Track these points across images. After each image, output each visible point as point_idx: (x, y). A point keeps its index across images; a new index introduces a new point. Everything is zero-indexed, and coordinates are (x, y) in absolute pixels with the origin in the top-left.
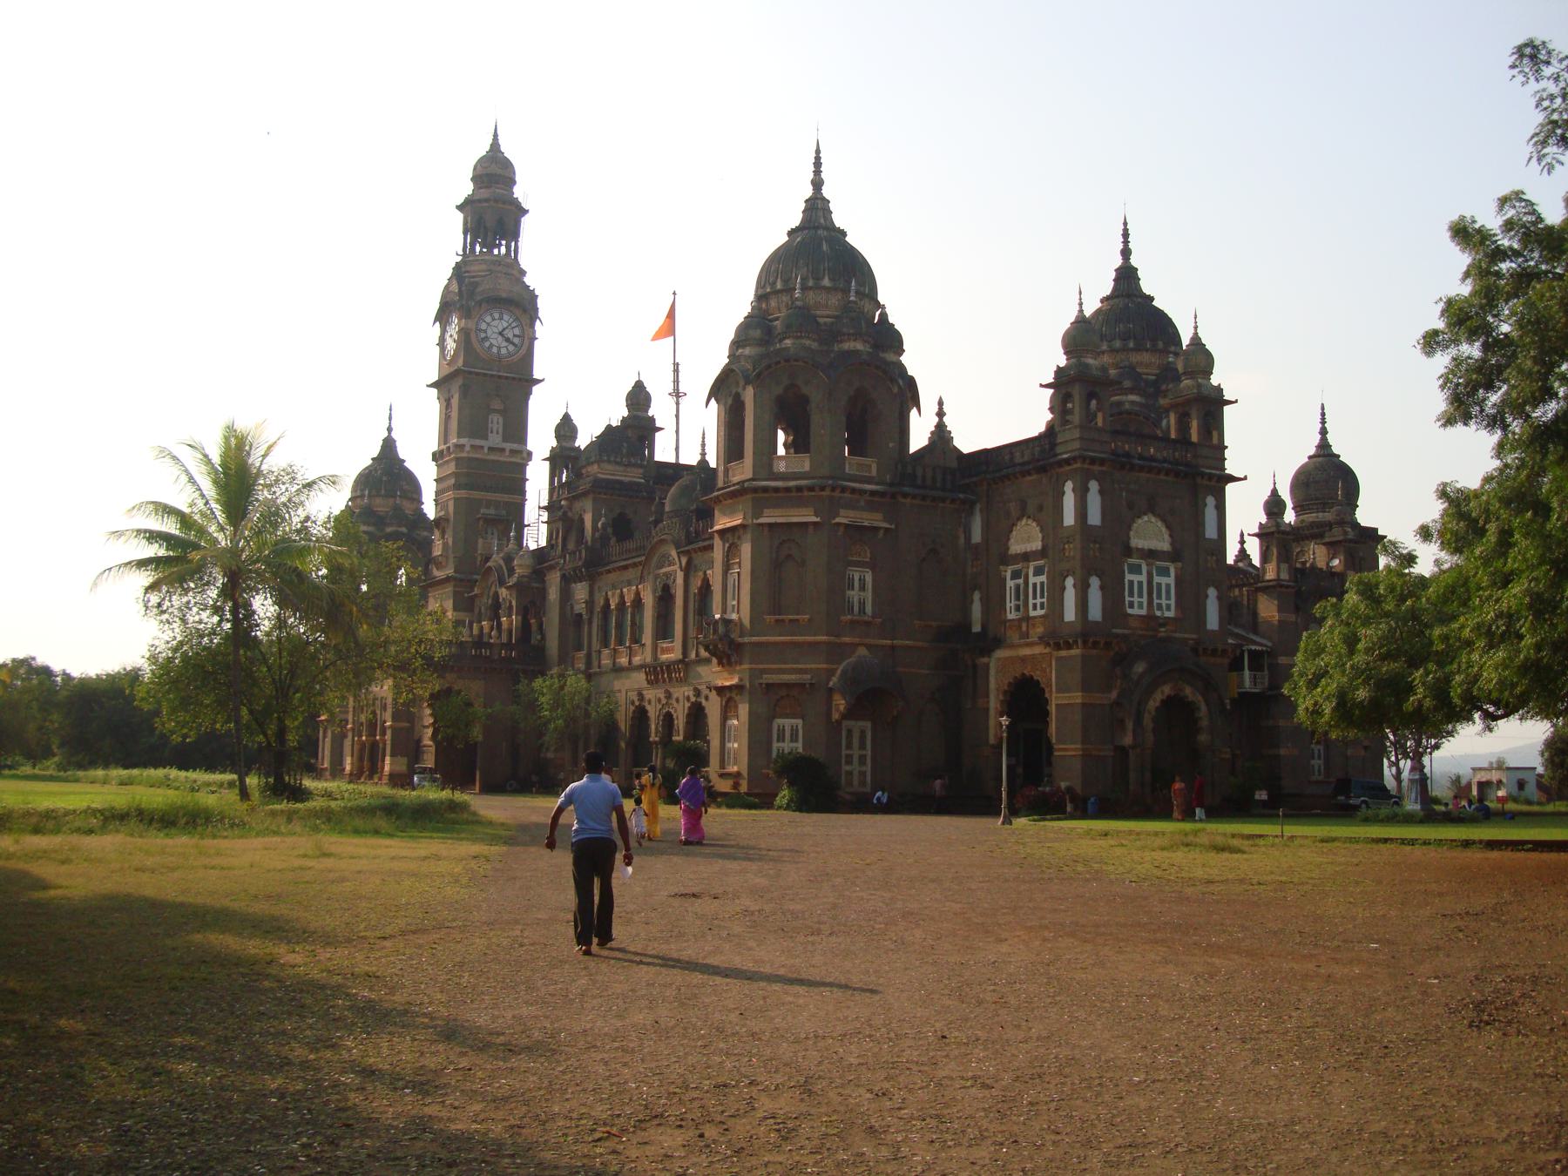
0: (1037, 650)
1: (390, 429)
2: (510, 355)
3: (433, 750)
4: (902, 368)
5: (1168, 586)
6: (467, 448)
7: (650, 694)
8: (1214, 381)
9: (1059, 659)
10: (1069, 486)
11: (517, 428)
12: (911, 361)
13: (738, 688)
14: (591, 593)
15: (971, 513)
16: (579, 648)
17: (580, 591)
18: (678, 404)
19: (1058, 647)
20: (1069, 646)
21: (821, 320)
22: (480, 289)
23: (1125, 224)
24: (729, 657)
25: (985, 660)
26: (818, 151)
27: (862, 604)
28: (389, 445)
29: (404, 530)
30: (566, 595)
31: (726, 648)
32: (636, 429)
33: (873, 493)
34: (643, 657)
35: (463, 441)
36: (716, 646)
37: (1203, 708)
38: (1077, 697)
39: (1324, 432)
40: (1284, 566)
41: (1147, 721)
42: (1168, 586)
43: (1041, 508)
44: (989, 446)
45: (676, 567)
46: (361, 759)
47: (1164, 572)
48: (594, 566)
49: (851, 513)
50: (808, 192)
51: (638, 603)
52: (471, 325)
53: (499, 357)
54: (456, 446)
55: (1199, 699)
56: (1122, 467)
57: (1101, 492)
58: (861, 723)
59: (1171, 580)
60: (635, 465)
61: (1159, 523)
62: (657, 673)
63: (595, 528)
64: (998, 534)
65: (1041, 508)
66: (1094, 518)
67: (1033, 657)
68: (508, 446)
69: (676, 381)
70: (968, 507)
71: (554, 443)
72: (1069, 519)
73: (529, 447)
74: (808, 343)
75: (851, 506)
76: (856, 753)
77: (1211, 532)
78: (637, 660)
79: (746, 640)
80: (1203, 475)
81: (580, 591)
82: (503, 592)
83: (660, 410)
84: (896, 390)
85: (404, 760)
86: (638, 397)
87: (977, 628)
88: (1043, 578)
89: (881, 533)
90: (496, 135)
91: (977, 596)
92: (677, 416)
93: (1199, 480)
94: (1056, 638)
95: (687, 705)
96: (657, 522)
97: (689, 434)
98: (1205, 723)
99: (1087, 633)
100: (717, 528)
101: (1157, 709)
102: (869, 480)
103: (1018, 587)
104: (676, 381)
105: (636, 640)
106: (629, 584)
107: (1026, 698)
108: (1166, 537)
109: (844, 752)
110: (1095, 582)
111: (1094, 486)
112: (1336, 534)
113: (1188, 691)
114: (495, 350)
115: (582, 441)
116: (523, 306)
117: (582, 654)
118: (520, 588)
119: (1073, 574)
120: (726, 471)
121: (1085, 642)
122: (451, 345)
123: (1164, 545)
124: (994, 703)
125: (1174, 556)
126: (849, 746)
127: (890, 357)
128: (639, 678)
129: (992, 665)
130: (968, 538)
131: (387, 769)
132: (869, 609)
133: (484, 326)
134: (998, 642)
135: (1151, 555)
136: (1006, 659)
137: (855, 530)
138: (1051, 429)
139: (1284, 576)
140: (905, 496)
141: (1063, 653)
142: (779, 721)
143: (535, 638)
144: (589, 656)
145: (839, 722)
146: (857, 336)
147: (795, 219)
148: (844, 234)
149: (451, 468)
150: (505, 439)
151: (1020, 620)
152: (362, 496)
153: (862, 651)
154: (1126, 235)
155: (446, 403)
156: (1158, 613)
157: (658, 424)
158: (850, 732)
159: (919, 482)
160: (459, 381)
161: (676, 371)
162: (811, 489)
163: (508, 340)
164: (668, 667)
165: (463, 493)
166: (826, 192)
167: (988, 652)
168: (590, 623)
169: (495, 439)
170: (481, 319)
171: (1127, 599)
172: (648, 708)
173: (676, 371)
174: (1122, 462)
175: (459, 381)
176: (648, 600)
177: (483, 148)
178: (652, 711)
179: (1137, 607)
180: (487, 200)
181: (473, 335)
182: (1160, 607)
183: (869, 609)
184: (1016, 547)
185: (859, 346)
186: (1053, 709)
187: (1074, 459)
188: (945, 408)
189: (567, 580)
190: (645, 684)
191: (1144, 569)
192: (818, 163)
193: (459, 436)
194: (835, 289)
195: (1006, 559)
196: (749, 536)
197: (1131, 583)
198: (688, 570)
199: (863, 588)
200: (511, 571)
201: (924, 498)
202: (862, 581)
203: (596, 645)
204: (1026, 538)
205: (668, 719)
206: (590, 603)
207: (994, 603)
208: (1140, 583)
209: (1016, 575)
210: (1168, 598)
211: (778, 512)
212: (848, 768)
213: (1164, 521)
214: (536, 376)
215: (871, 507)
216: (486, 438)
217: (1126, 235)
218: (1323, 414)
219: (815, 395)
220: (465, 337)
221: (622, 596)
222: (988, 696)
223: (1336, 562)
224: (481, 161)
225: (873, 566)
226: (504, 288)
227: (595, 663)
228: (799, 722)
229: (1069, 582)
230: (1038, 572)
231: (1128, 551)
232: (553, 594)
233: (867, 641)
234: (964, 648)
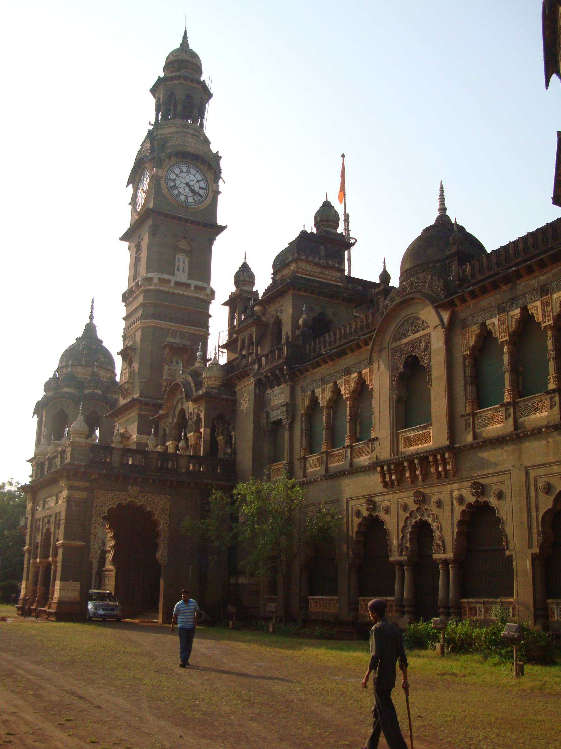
1: (91, 318)
3: (113, 574)
6: (155, 280)
11: (202, 268)
14: (293, 395)
16: (276, 458)
22: (168, 144)
28: (90, 329)
29: (99, 392)
30: (260, 402)
35: (151, 275)
46: (35, 584)
48: (298, 362)
51: (362, 391)
52: (161, 173)
53: (185, 206)
54: (145, 279)
62: (397, 471)
63: (295, 326)
68: (194, 283)
71: (233, 289)
73: (214, 284)
78: (364, 460)
82: (190, 406)
85: (77, 585)
95: (458, 509)
114: (182, 198)
116: (209, 165)
117: (282, 465)
118: (209, 399)
122: (141, 197)
131: (56, 595)
133: (173, 176)
143: (223, 452)
149: (140, 299)
150: (190, 278)
152: (67, 366)
155: (136, 250)
160: (150, 222)
163: (193, 191)
165: (150, 322)
169: (182, 276)
170: (170, 170)
178: (393, 523)
180: (178, 78)
181: (163, 182)
189: (263, 385)
190: (380, 488)
193: (148, 270)
198: (450, 330)
200: (199, 385)
203: (299, 451)
205: (422, 532)
214: (220, 221)
216: (173, 275)
220: (156, 188)
221: (336, 391)
226: (192, 146)
232: (246, 402)
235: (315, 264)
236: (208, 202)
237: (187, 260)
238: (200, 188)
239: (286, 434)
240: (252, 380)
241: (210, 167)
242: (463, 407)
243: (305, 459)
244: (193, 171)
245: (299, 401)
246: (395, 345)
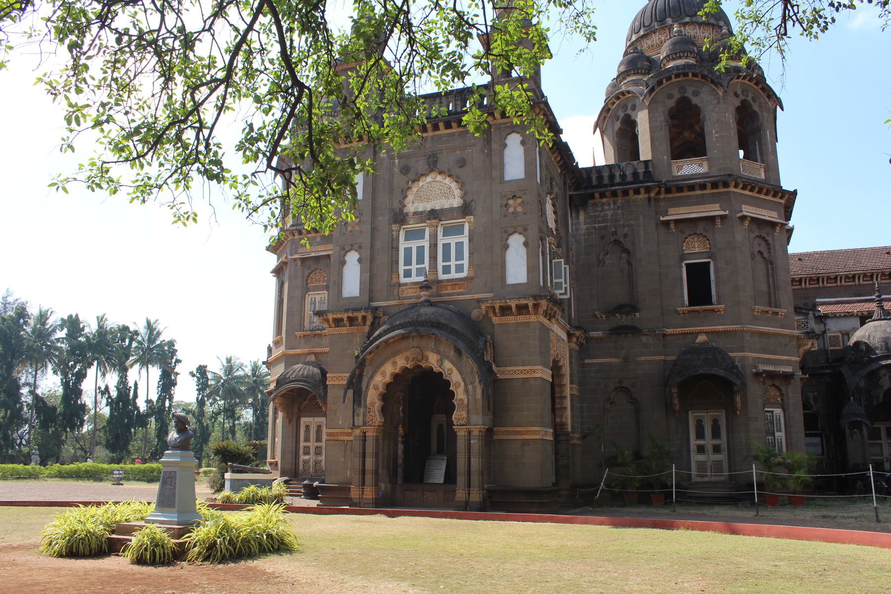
5: (459, 245)
41: (373, 397)
42: (459, 245)
47: (459, 230)
55: (447, 365)
59: (465, 239)
61: (448, 181)
76: (312, 444)
98: (460, 394)
108: (457, 192)
109: (302, 444)
113: (433, 360)
125: (465, 210)
126: (307, 439)
135: (434, 215)
158: (307, 427)
171: (402, 268)
179: (411, 274)
197: (408, 251)
208: (420, 249)
212: (307, 457)
231: (400, 218)
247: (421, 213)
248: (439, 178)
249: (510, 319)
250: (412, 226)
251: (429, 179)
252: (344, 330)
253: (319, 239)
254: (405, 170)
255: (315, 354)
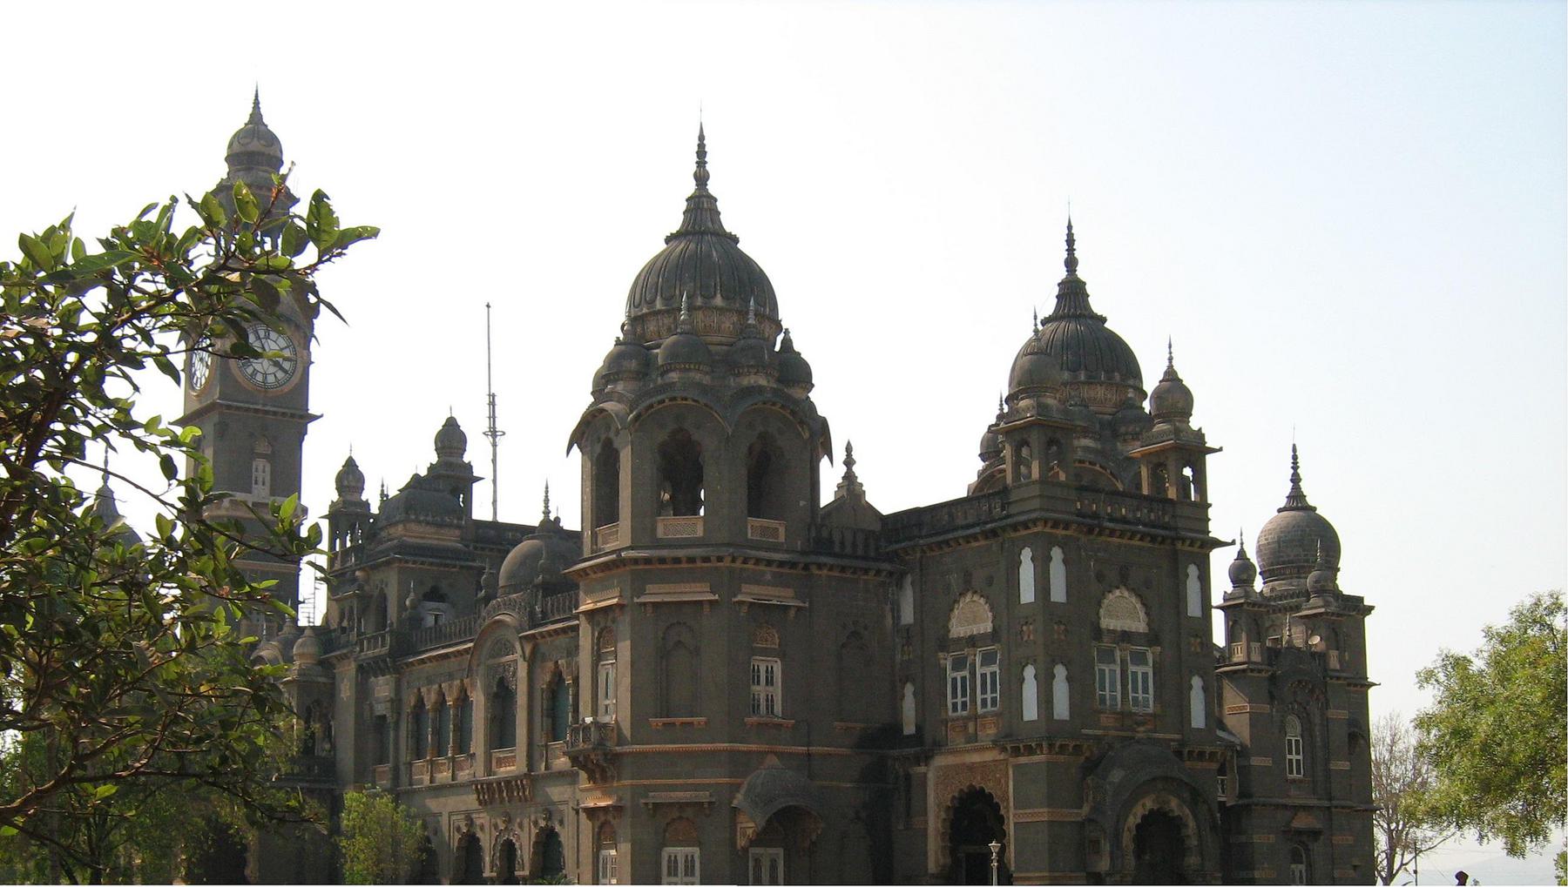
0: (989, 756)
2: (279, 383)
4: (812, 407)
5: (1145, 675)
7: (482, 819)
8: (1194, 423)
9: (1017, 767)
10: (1026, 555)
11: (288, 479)
12: (823, 398)
13: (617, 809)
15: (900, 585)
16: (382, 760)
17: (382, 687)
18: (494, 445)
19: (1016, 752)
20: (1030, 751)
21: (711, 348)
23: (1070, 227)
24: (603, 771)
25: (922, 769)
26: (701, 138)
27: (770, 701)
30: (363, 692)
31: (600, 761)
32: (449, 476)
33: (781, 564)
34: (472, 771)
36: (587, 758)
37: (1192, 824)
38: (1042, 814)
39: (1296, 479)
40: (1255, 645)
41: (1127, 839)
42: (1145, 675)
43: (990, 581)
44: (922, 505)
45: (518, 655)
47: (1140, 659)
49: (756, 589)
50: (690, 188)
51: (464, 701)
53: (265, 386)
56: (1091, 531)
57: (1065, 561)
58: (771, 851)
60: (450, 526)
61: (1134, 599)
62: (489, 793)
64: (935, 612)
65: (990, 581)
66: (1058, 594)
67: (984, 765)
69: (493, 417)
70: (898, 579)
71: (335, 497)
72: (1027, 594)
74: (698, 376)
75: (757, 580)
77: (1194, 609)
78: (464, 775)
79: (627, 749)
80: (1183, 540)
81: (382, 687)
83: (476, 454)
84: (806, 435)
86: (451, 439)
87: (909, 729)
88: (995, 668)
89: (792, 613)
90: (256, 103)
91: (909, 689)
92: (494, 461)
93: (1179, 545)
94: (1014, 741)
95: (534, 831)
96: (487, 599)
97: (533, 481)
99: (1052, 735)
100: (582, 608)
101: (1138, 827)
102: (775, 548)
103: (963, 679)
104: (493, 417)
105: (462, 746)
106: (451, 677)
107: (976, 816)
108: (1142, 615)
110: (1060, 672)
111: (1057, 553)
112: (1314, 606)
113: (1174, 805)
114: (259, 378)
115: (372, 497)
117: (385, 768)
119: (1034, 662)
120: (594, 536)
121: (1051, 746)
123: (1139, 625)
124: (934, 822)
125: (1153, 638)
127: (796, 393)
128: (470, 801)
129: (930, 775)
130: (897, 617)
132: (778, 708)
134: (938, 746)
135: (1126, 636)
136: (947, 767)
137: (761, 610)
138: (985, 479)
139: (1256, 657)
140: (820, 566)
141: (1023, 760)
142: (669, 851)
143: (322, 748)
144: (396, 769)
145: (745, 850)
146: (760, 367)
147: (675, 223)
148: (735, 240)
151: (968, 718)
153: (774, 761)
154: (1070, 241)
156: (1134, 709)
157: (476, 473)
158: (757, 861)
159: (837, 549)
160: (214, 417)
161: (492, 404)
162: (706, 559)
164: (508, 782)
166: (713, 188)
167: (926, 758)
168: (397, 724)
172: (479, 834)
173: (492, 404)
174: (1091, 525)
175: (214, 417)
176: (478, 698)
177: (240, 120)
178: (486, 840)
182: (1135, 699)
183: (778, 708)
184: (958, 629)
185: (763, 382)
186: (1011, 829)
187: (1035, 522)
188: (855, 455)
189: (366, 671)
190: (476, 805)
191: (1118, 654)
192: (701, 153)
194: (729, 310)
195: (944, 643)
196: (627, 618)
199: (770, 682)
201: (843, 569)
202: (770, 672)
203: (405, 756)
204: (971, 617)
206: (396, 702)
207: (929, 701)
209: (959, 664)
210: (1146, 691)
211: (666, 588)
213: (1139, 596)
214: (313, 410)
215: (779, 581)
217: (1070, 241)
218: (1295, 457)
219: (709, 444)
221: (441, 695)
222: (926, 814)
223: (1316, 640)
224: (238, 136)
225: (782, 655)
227: (404, 779)
228: (696, 851)
229: (1029, 672)
230: (988, 659)
231: (1098, 633)
232: (346, 691)
233: (780, 748)
234: (888, 755)
235: (428, 523)
236: (296, 379)
237: (268, 469)
238: (286, 359)
239: (392, 734)
240: (353, 665)
241: (298, 327)
242: (540, 739)
243: (411, 764)
244: (273, 335)
245: (405, 698)
246: (491, 662)
247: (1114, 631)
248: (1126, 594)
249: (1199, 765)
250: (1106, 643)
251: (1117, 593)
252: (1062, 758)
253: (768, 577)
254: (1100, 577)
255: (775, 753)
